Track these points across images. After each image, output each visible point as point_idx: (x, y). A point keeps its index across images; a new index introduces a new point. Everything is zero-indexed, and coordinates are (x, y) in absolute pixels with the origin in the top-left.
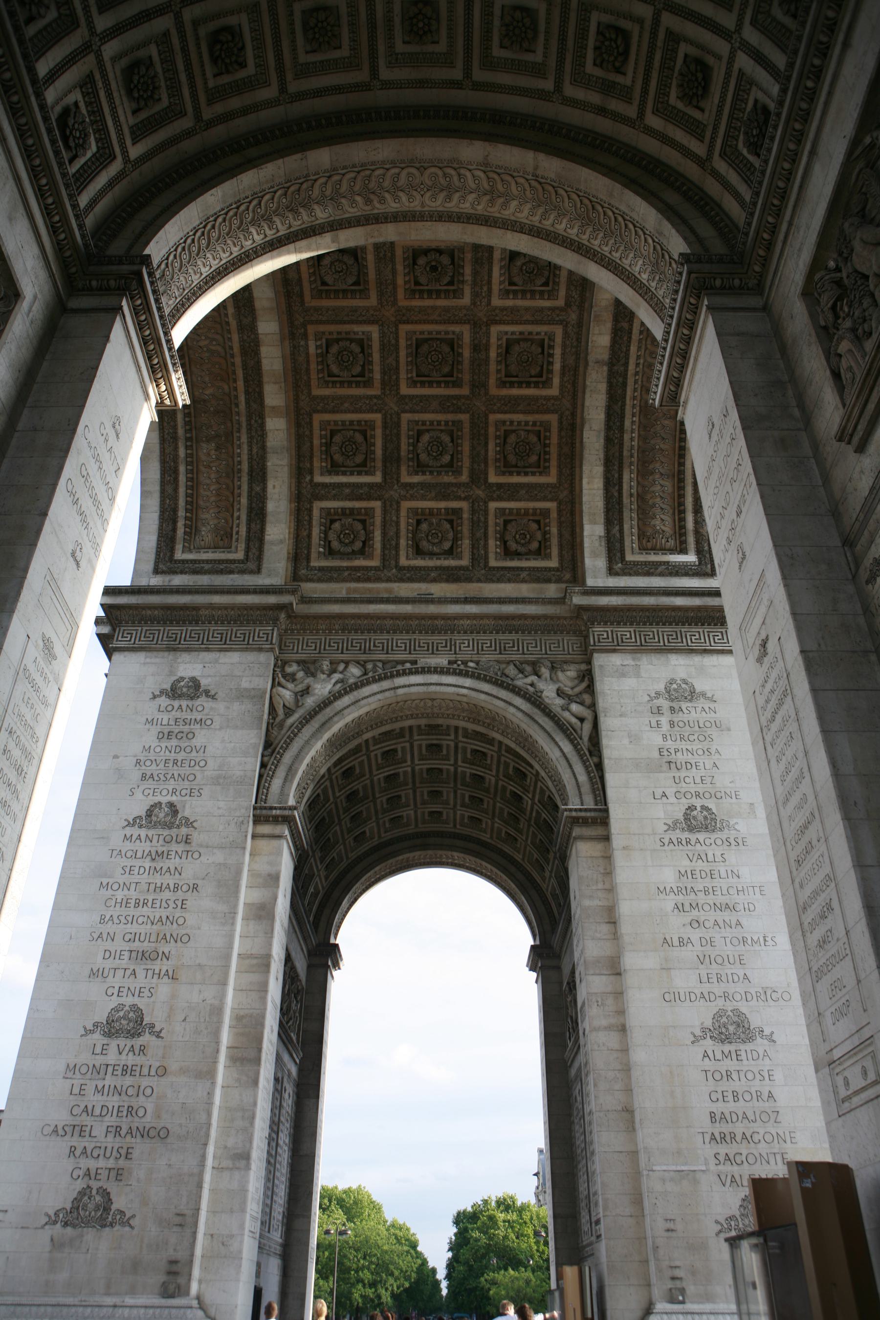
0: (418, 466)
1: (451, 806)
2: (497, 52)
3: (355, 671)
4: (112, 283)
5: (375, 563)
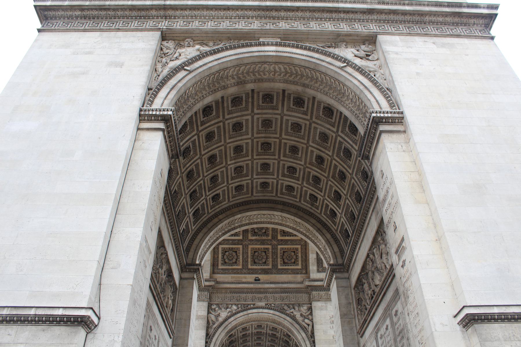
0: (254, 233)
1: (264, 341)
2: (284, 191)
3: (234, 307)
4: (192, 270)
5: (240, 267)
